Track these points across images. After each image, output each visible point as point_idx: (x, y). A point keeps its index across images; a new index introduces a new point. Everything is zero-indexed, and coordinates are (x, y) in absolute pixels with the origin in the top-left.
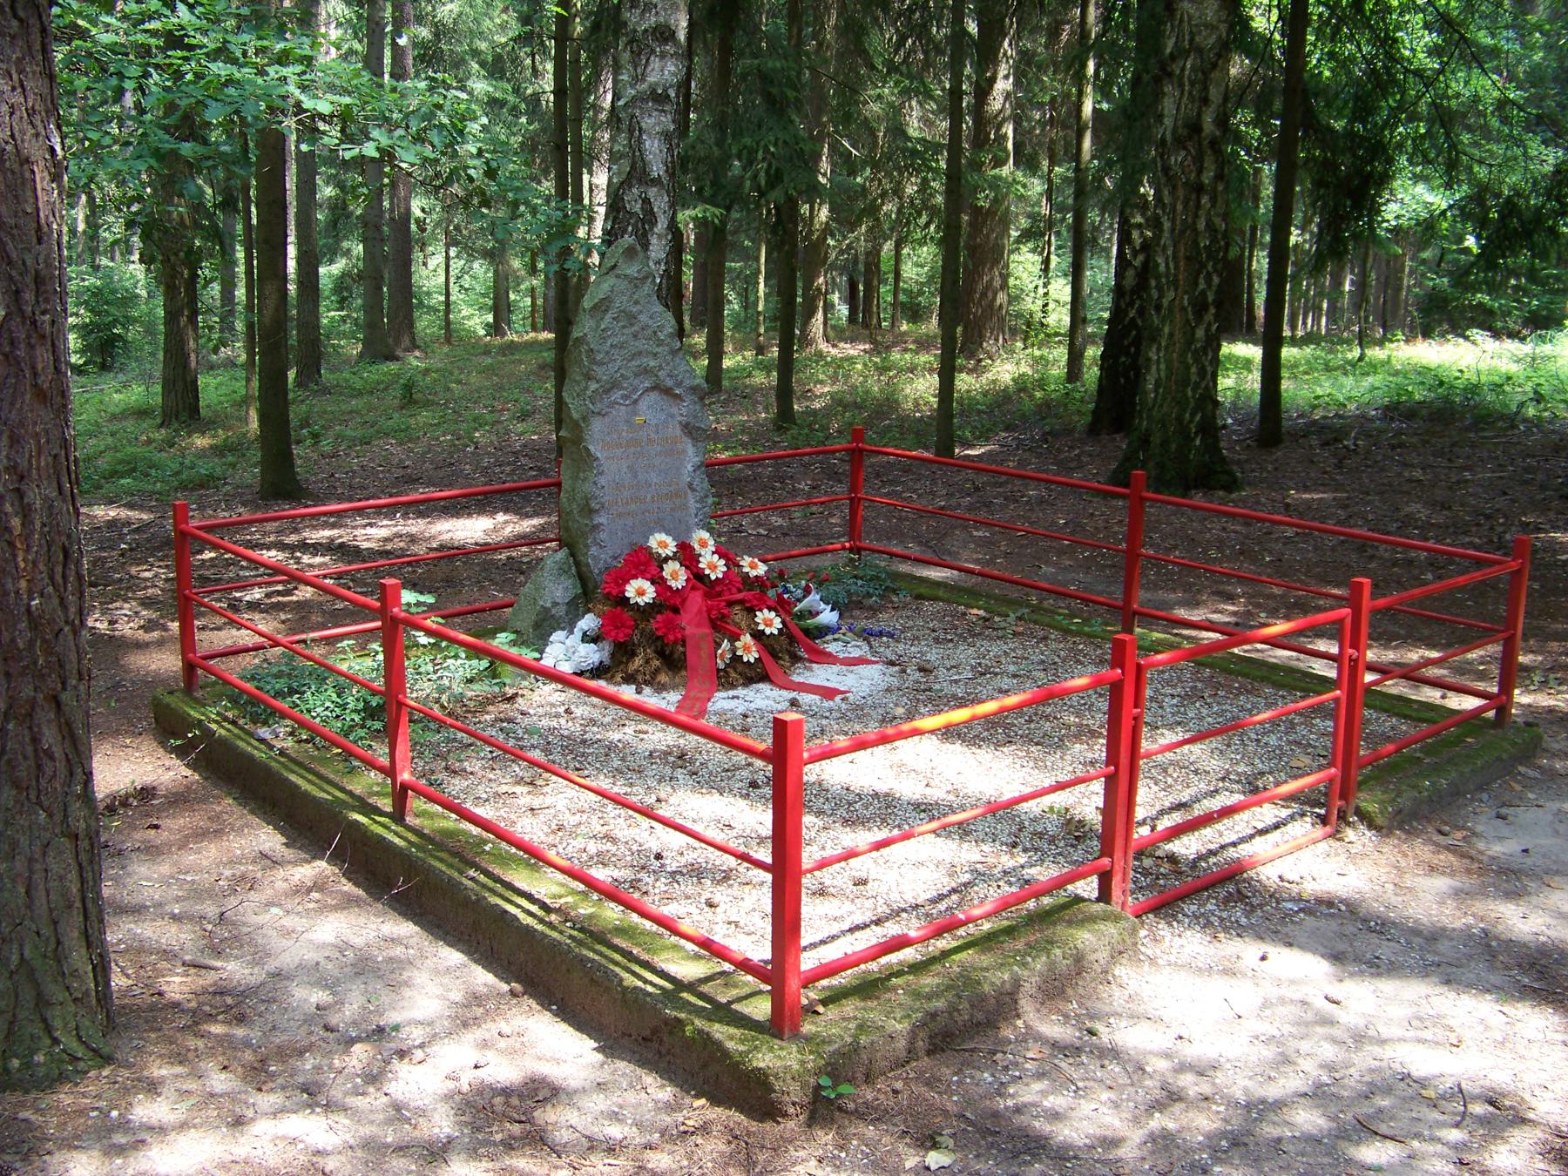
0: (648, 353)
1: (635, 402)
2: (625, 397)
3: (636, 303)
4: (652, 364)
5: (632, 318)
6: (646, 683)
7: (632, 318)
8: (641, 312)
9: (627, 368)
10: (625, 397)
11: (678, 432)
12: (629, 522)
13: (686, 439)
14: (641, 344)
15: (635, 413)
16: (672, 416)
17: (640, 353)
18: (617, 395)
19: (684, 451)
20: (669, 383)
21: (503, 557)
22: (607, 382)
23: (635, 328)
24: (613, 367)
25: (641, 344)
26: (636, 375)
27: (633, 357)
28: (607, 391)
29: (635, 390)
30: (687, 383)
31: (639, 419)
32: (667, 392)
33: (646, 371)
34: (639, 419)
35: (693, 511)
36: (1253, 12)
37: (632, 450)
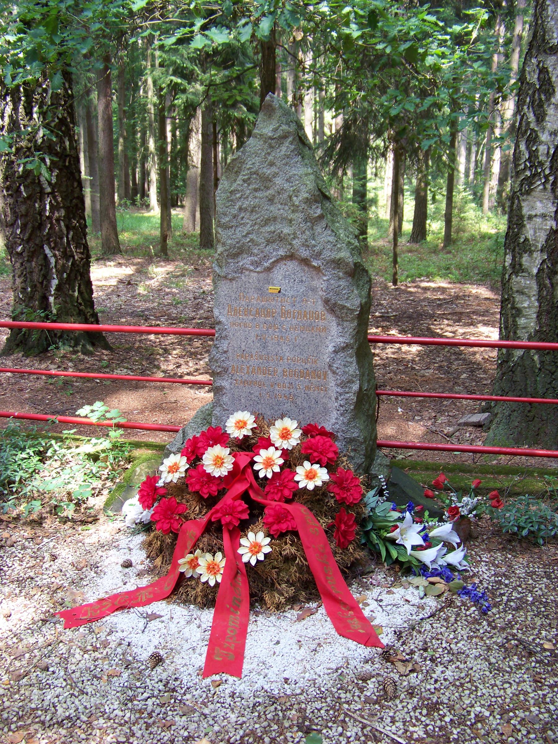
0: (283, 219)
1: (269, 270)
2: (257, 264)
3: (272, 164)
4: (286, 230)
5: (266, 181)
6: (353, 572)
7: (266, 181)
8: (275, 175)
9: (258, 233)
10: (257, 264)
11: (320, 307)
12: (255, 390)
13: (330, 317)
14: (276, 210)
15: (269, 282)
16: (314, 290)
17: (275, 219)
18: (246, 261)
19: (325, 329)
20: (304, 253)
21: (393, 332)
22: (232, 247)
23: (271, 192)
24: (240, 232)
25: (276, 210)
26: (269, 242)
27: (267, 222)
28: (235, 256)
29: (266, 257)
30: (327, 254)
31: (273, 289)
32: (305, 262)
33: (281, 238)
34: (273, 289)
35: (334, 395)
36: (406, 187)
37: (262, 319)
